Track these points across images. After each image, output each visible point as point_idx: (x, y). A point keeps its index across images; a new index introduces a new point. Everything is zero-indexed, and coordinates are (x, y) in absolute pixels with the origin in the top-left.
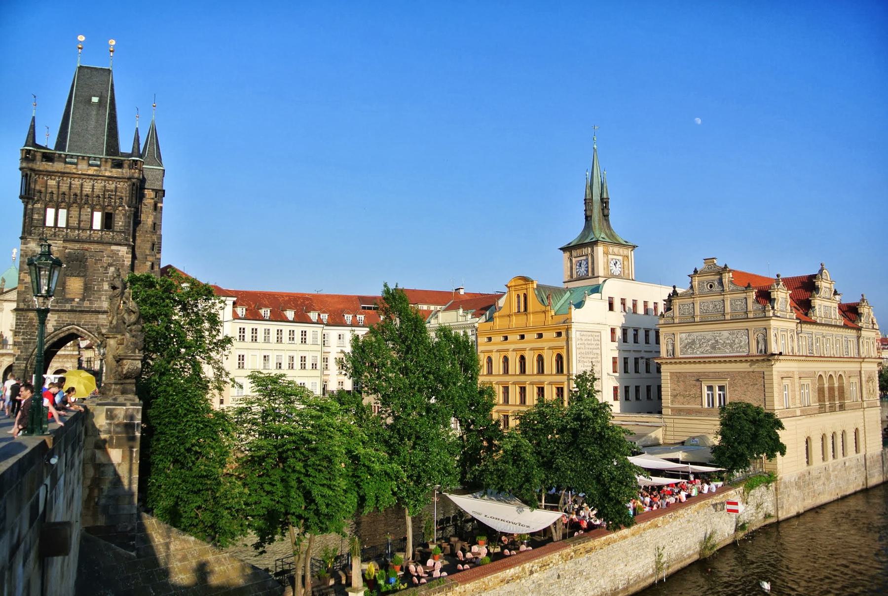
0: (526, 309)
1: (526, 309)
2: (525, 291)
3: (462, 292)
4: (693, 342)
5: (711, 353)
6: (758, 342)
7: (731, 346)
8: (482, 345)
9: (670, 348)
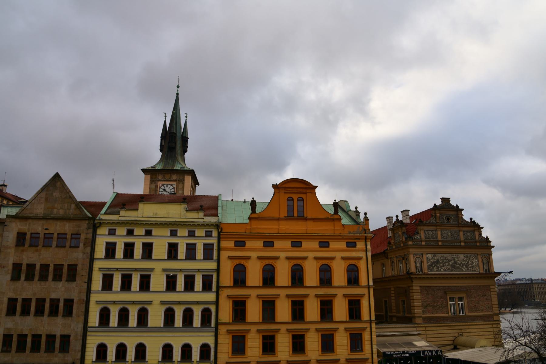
4: (438, 262)
5: (452, 271)
6: (484, 264)
7: (467, 266)
8: (227, 249)
9: (418, 265)
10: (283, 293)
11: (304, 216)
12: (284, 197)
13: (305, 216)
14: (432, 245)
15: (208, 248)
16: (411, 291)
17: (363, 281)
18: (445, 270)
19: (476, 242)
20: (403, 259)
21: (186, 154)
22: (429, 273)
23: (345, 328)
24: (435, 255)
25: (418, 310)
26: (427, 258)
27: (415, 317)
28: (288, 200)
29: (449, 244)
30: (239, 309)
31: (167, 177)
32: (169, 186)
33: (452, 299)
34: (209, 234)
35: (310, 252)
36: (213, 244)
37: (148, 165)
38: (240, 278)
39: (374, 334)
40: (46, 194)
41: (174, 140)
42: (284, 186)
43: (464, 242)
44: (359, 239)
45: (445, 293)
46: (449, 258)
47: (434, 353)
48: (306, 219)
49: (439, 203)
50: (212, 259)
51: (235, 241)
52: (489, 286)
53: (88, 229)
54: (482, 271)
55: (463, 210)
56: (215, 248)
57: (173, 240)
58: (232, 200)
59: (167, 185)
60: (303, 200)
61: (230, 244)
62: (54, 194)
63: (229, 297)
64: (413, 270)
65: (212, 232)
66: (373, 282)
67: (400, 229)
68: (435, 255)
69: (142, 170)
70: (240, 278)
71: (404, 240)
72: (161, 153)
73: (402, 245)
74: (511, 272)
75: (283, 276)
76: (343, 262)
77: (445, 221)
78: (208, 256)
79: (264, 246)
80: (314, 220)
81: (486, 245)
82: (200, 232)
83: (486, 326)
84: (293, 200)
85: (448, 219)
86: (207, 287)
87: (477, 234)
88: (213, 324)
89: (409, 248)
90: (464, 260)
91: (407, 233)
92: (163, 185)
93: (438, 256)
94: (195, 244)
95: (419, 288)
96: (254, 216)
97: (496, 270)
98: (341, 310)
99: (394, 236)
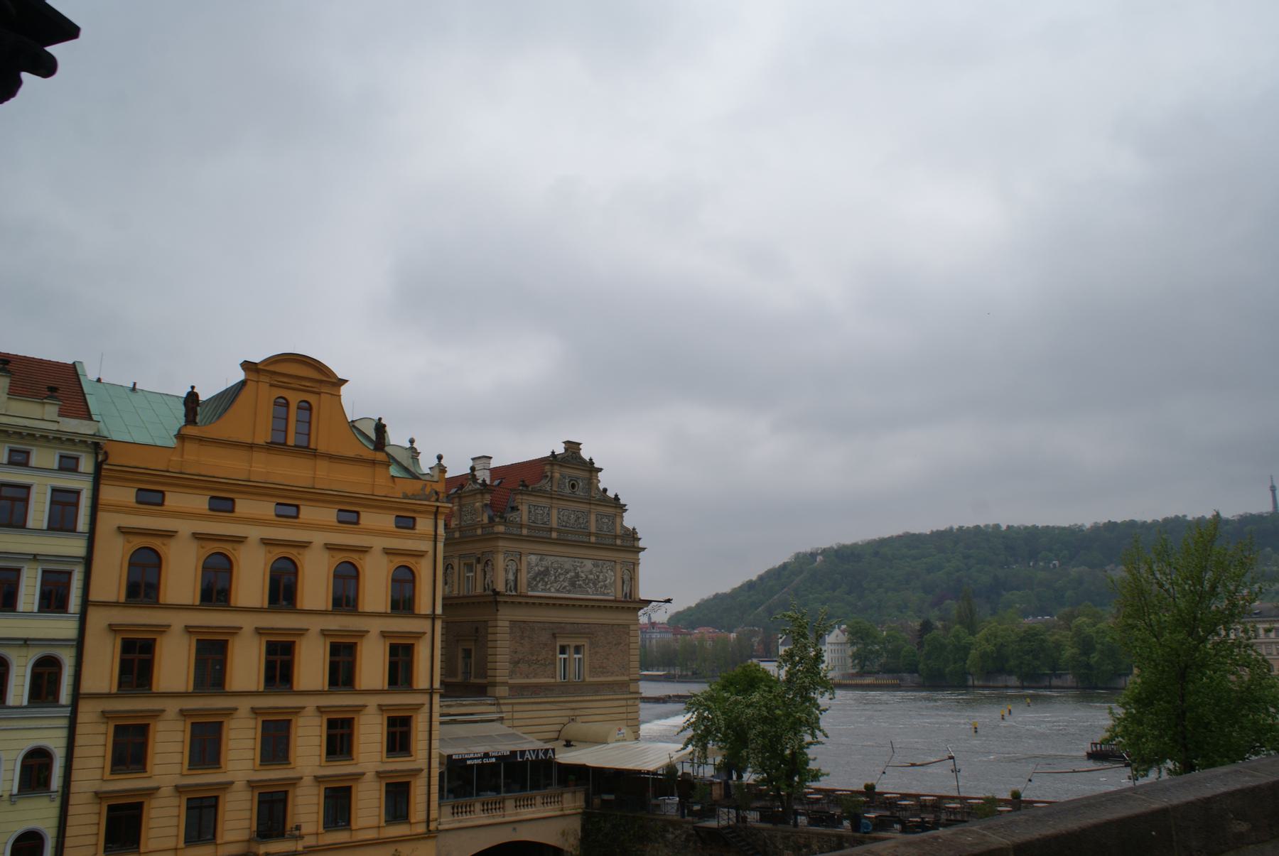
4: (546, 572)
5: (569, 592)
7: (595, 585)
9: (511, 577)
10: (248, 623)
11: (308, 447)
12: (266, 393)
13: (312, 446)
14: (540, 536)
15: (63, 502)
16: (490, 630)
17: (423, 603)
18: (558, 591)
19: (616, 537)
20: (478, 561)
22: (530, 593)
23: (380, 706)
24: (542, 556)
25: (502, 668)
26: (529, 564)
27: (494, 684)
28: (276, 403)
29: (570, 537)
30: (137, 661)
33: (563, 651)
34: (68, 465)
35: (318, 531)
36: (77, 493)
38: (143, 585)
39: (436, 718)
42: (271, 368)
43: (597, 535)
44: (420, 512)
45: (554, 636)
46: (567, 566)
47: (541, 754)
48: (314, 454)
49: (560, 450)
50: (73, 530)
51: (212, 498)
52: (628, 626)
54: (620, 596)
55: (601, 470)
58: (99, 380)
60: (310, 408)
61: (127, 495)
63: (113, 629)
64: (500, 587)
65: (77, 459)
66: (444, 606)
67: (479, 496)
68: (542, 556)
70: (143, 585)
71: (486, 520)
73: (479, 532)
74: (668, 601)
75: (250, 584)
76: (384, 559)
77: (568, 490)
78: (61, 521)
79: (211, 509)
80: (331, 457)
81: (629, 543)
82: (44, 457)
83: (616, 703)
84: (287, 404)
85: (573, 486)
86: (53, 600)
87: (618, 520)
88: (65, 695)
89: (498, 538)
90: (591, 573)
91: (491, 506)
93: (548, 561)
94: (27, 488)
95: (507, 624)
96: (191, 430)
97: (643, 595)
98: (372, 666)
99: (460, 510)
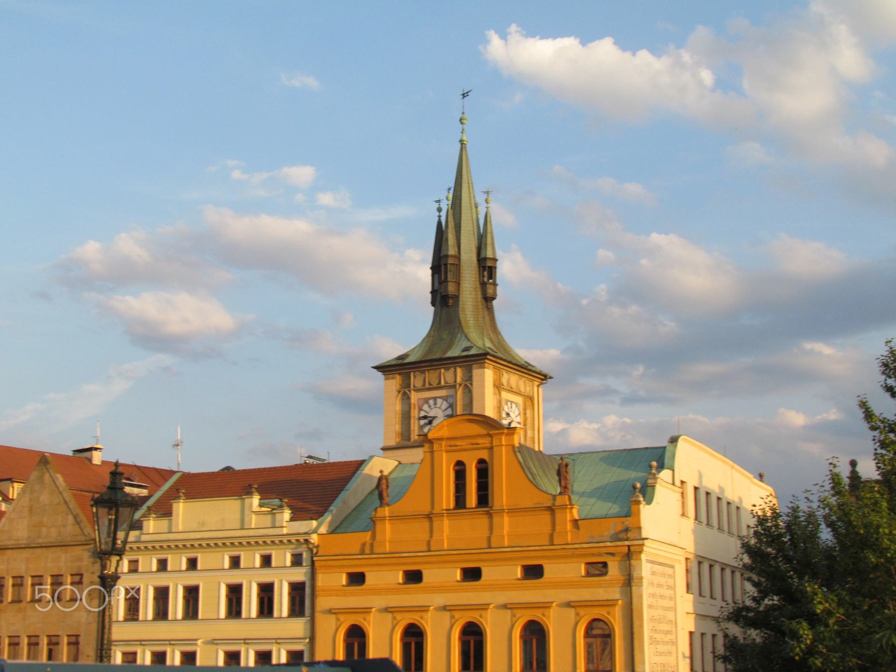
0: (484, 499)
1: (484, 499)
2: (484, 455)
3: (97, 458)
8: (330, 592)
21: (495, 303)
31: (431, 376)
32: (439, 401)
37: (391, 351)
40: (30, 500)
41: (459, 273)
53: (94, 563)
56: (308, 590)
57: (235, 577)
59: (435, 399)
62: (42, 498)
69: (376, 368)
72: (433, 308)
92: (426, 401)
